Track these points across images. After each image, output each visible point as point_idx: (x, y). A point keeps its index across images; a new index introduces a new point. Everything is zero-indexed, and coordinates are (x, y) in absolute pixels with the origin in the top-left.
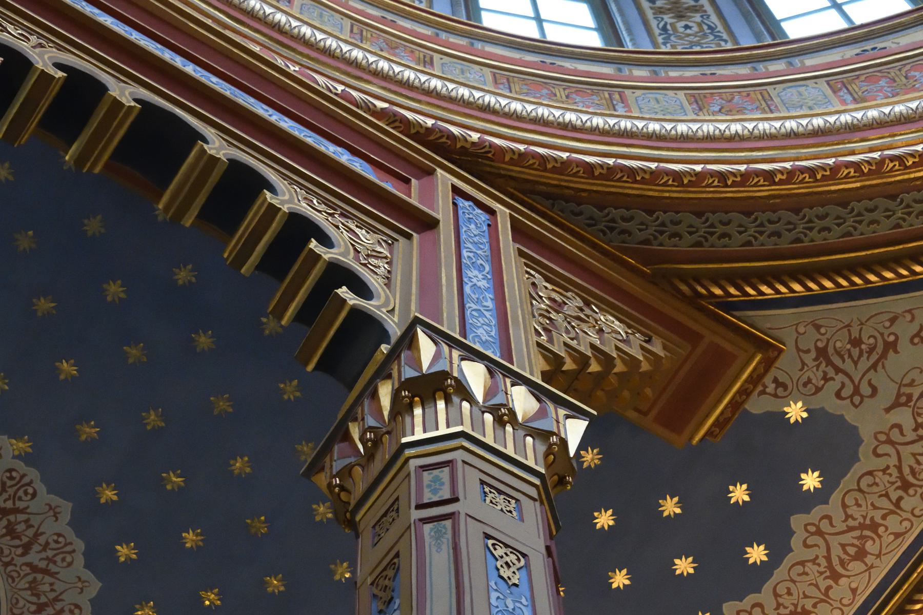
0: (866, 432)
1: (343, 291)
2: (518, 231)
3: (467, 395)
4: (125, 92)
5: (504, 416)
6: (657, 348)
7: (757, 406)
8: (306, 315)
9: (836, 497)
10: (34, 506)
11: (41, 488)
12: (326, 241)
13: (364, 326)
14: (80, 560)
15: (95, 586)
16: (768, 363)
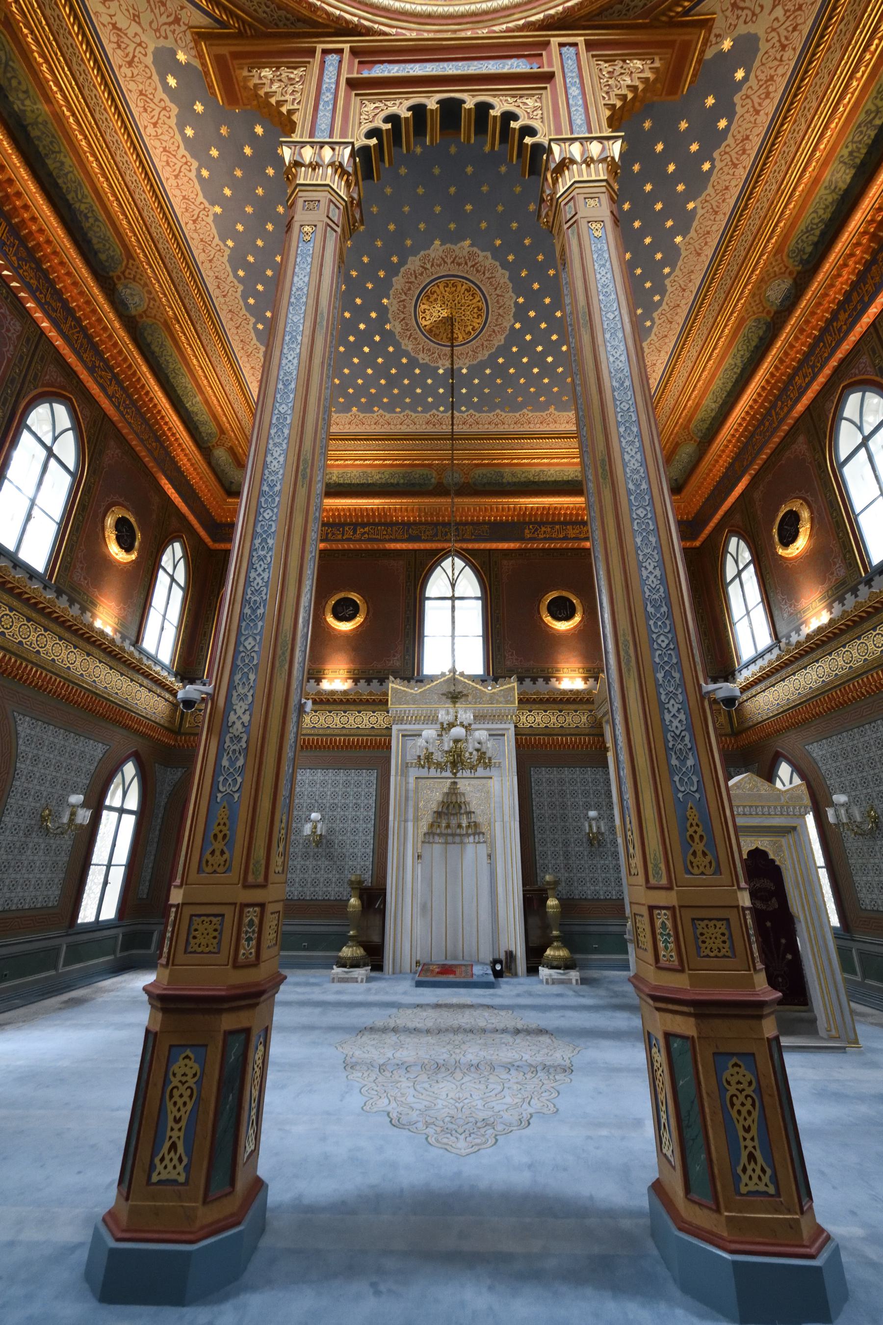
0: (762, 34)
1: (528, 140)
2: (589, 45)
3: (572, 161)
4: (432, 103)
5: (588, 161)
6: (657, 64)
7: (709, 54)
8: (519, 155)
9: (752, 75)
10: (480, 259)
11: (479, 252)
12: (515, 117)
13: (538, 148)
14: (499, 268)
15: (507, 274)
16: (710, 31)
